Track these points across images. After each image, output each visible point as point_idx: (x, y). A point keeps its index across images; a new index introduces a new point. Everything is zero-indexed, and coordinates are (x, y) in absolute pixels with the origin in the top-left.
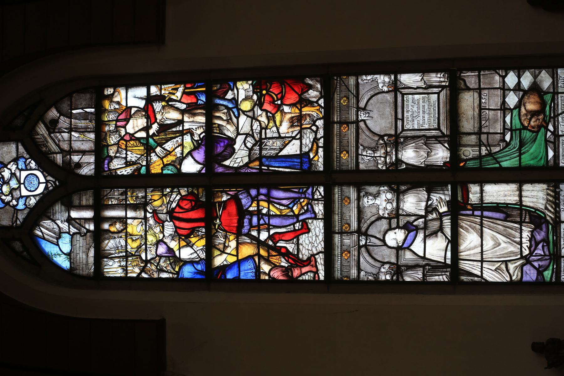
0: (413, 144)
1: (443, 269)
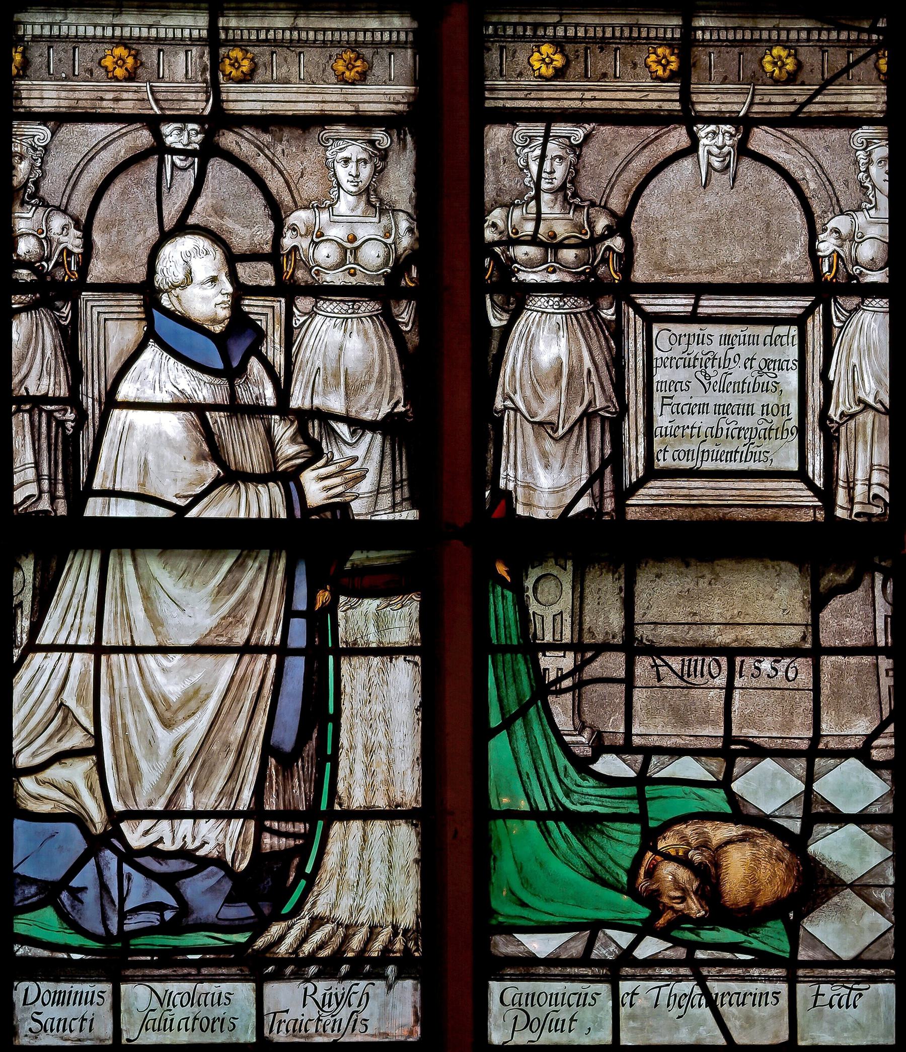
0: (588, 363)
1: (65, 483)
